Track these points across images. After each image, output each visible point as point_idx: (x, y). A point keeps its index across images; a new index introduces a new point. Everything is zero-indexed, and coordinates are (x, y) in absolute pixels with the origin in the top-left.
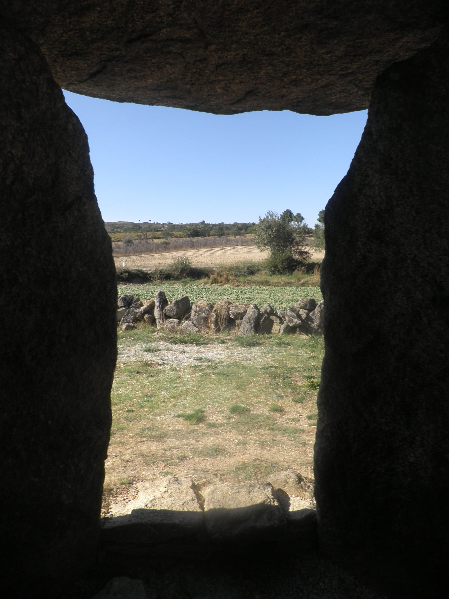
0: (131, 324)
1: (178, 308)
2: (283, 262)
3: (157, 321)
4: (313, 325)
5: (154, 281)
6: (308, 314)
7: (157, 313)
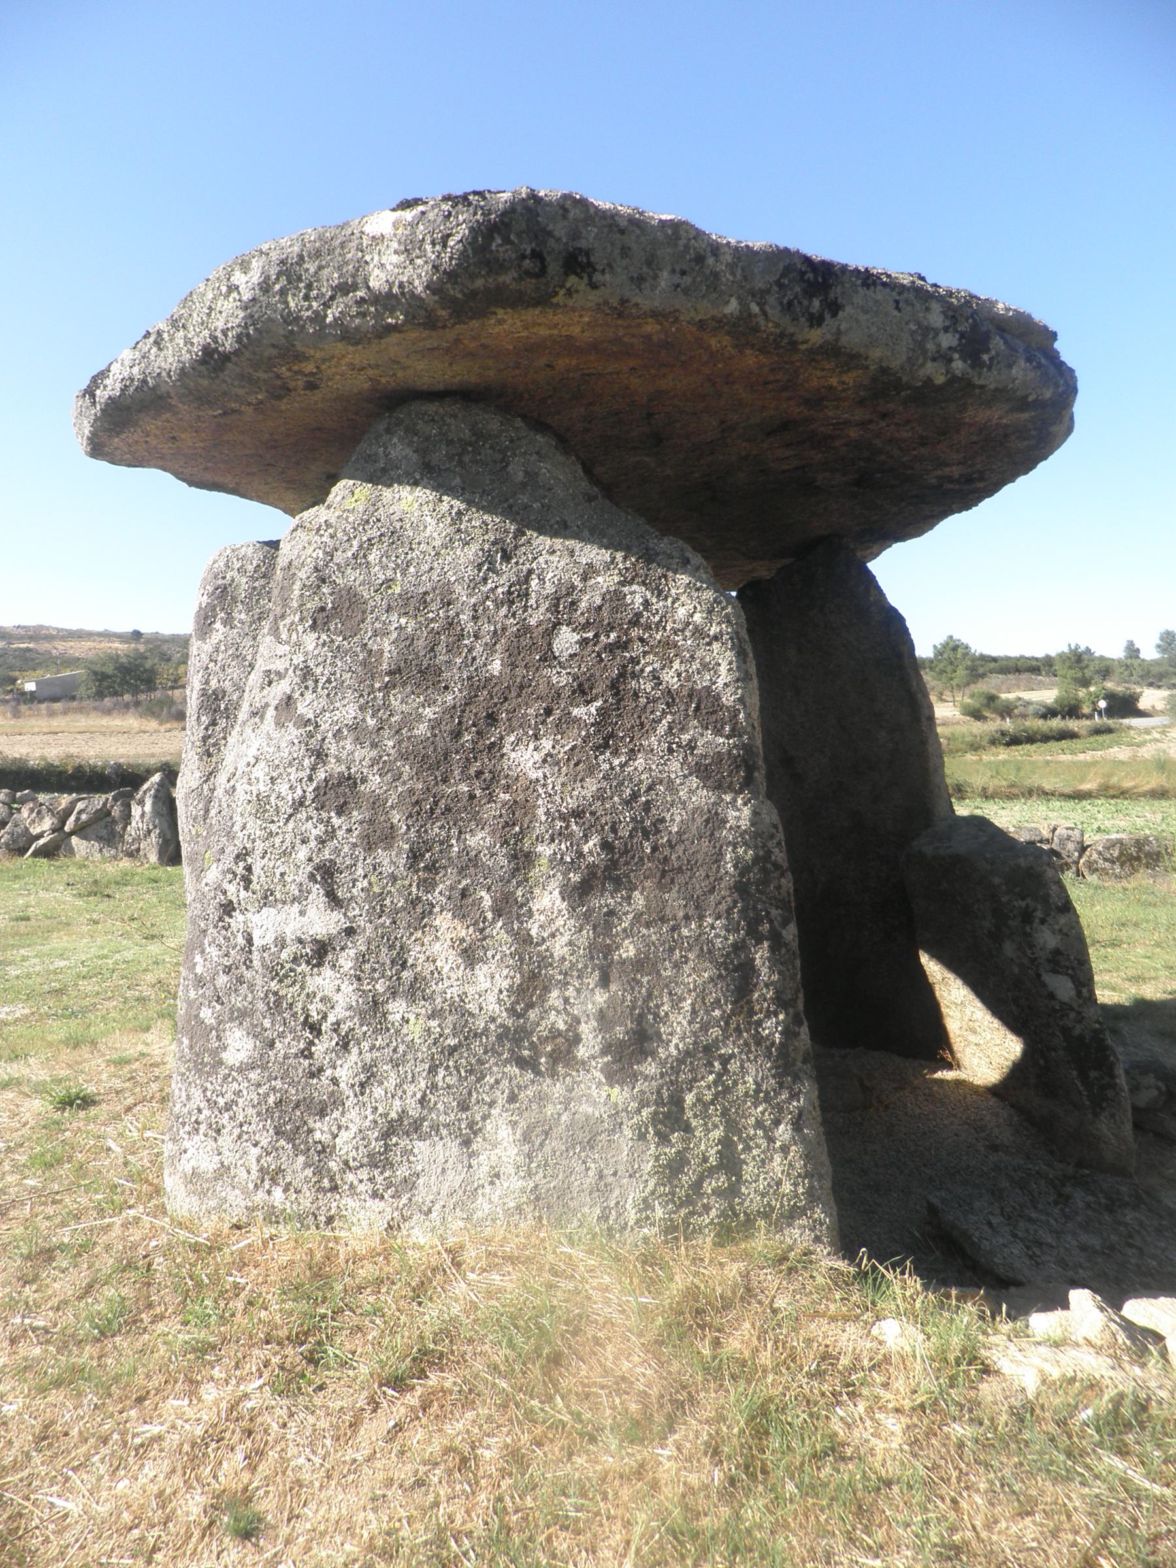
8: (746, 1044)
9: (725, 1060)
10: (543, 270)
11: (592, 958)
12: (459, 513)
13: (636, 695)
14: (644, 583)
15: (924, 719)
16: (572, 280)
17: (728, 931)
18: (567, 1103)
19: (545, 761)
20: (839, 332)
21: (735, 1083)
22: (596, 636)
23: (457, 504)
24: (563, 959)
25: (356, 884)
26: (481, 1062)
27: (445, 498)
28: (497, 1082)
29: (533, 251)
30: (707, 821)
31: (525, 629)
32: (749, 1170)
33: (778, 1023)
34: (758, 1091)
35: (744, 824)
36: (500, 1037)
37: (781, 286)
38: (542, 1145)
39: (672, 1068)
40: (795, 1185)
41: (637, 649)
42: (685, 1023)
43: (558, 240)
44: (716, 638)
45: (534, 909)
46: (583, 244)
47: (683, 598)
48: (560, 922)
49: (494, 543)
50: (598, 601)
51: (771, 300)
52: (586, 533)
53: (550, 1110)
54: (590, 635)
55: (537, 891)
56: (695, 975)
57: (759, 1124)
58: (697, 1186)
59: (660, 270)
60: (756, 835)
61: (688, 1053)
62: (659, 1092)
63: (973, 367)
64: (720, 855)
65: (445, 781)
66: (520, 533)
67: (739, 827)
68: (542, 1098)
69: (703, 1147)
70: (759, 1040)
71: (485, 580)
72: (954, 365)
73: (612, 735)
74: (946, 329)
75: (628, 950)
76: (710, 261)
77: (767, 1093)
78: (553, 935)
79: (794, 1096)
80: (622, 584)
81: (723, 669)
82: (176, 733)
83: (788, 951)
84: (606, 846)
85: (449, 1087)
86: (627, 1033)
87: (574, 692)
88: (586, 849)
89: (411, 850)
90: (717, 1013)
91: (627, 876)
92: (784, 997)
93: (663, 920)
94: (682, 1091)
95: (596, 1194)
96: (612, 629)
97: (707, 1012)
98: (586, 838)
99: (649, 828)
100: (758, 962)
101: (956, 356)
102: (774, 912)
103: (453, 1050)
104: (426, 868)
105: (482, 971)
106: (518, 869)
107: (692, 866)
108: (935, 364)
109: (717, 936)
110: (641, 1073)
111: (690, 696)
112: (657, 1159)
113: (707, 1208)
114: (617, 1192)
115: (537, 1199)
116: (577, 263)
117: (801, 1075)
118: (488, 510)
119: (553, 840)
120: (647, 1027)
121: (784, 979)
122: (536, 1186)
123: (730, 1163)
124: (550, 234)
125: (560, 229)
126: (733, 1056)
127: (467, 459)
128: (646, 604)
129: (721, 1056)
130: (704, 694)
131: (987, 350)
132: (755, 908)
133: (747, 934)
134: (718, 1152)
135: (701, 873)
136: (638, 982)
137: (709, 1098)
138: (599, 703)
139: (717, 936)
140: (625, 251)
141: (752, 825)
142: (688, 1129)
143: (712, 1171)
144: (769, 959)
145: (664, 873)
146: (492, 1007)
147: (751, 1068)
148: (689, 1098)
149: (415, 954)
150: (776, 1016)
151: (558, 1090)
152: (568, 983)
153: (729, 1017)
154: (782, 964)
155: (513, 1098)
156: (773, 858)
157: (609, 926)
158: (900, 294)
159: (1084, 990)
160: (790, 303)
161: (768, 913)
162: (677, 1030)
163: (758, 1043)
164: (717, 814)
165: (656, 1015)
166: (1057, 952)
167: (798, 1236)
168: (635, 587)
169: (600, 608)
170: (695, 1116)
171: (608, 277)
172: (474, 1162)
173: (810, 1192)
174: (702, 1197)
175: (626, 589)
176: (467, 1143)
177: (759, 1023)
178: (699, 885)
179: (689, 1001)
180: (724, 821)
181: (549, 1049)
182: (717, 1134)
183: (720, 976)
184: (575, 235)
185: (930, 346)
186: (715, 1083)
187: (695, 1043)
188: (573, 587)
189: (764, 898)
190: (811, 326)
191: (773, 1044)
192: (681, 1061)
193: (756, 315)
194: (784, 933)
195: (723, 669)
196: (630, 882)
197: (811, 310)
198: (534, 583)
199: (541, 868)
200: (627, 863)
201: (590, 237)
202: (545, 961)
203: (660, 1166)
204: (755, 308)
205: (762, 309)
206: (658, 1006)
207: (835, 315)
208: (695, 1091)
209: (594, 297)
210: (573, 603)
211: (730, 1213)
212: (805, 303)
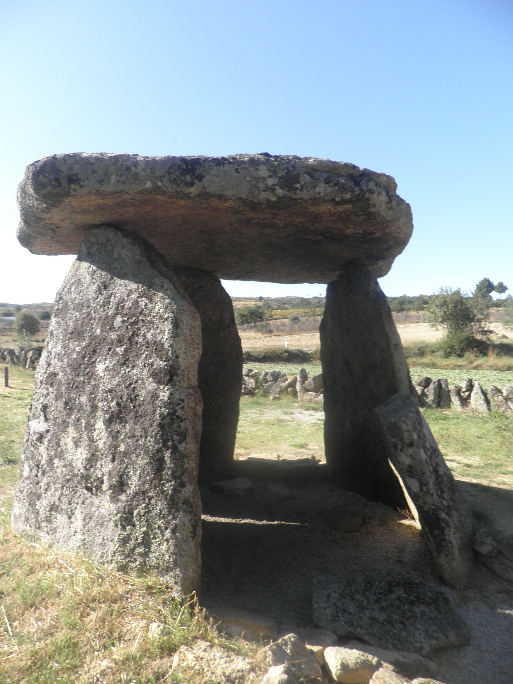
0: (277, 396)
1: (315, 383)
2: (461, 343)
3: (298, 394)
4: (427, 400)
5: (314, 362)
6: (423, 391)
7: (298, 387)
8: (158, 493)
9: (150, 498)
10: (60, 185)
11: (110, 450)
12: (95, 272)
13: (137, 343)
14: (146, 297)
15: (392, 347)
16: (73, 186)
18: (98, 507)
19: (106, 369)
20: (204, 187)
21: (153, 509)
22: (128, 319)
23: (95, 268)
24: (102, 449)
25: (52, 414)
26: (76, 487)
27: (92, 266)
28: (80, 495)
29: (54, 178)
30: (152, 396)
31: (107, 316)
32: (153, 547)
33: (171, 485)
34: (160, 513)
35: (166, 398)
36: (82, 477)
37: (169, 173)
38: (88, 523)
39: (131, 499)
40: (170, 557)
41: (141, 324)
42: (137, 480)
43: (64, 172)
44: (166, 319)
45: (96, 428)
46: (74, 172)
47: (159, 303)
48: (103, 434)
49: (102, 283)
50: (131, 305)
51: (165, 179)
52: (131, 277)
53: (93, 509)
54: (126, 319)
55: (98, 421)
56: (142, 461)
58: (133, 550)
59: (111, 176)
60: (170, 403)
61: (137, 493)
62: (124, 508)
63: (289, 191)
64: (155, 411)
65: (78, 376)
66: (112, 278)
67: (163, 400)
68: (92, 504)
69: (137, 534)
70: (163, 491)
71: (98, 297)
72: (277, 191)
73: (128, 360)
74: (270, 177)
75: (122, 448)
76: (133, 169)
77: (164, 515)
78: (100, 439)
79: (174, 518)
80: (138, 297)
81: (166, 333)
82: (267, 338)
83: (180, 454)
84: (118, 404)
85: (66, 495)
86: (116, 482)
87: (117, 342)
88: (112, 405)
89: (65, 402)
90: (148, 478)
91: (124, 417)
92: (175, 474)
93: (134, 436)
94: (133, 509)
95: (101, 546)
96: (134, 316)
97: (145, 477)
98: (112, 400)
99: (133, 399)
100: (166, 458)
101: (277, 187)
102: (175, 437)
103: (68, 480)
104: (69, 409)
105: (79, 450)
106: (92, 412)
107: (145, 415)
108: (266, 193)
109: (151, 445)
110: (120, 499)
111: (154, 343)
112: (119, 535)
113: (136, 560)
114: (108, 547)
115: (84, 544)
116: (72, 179)
117: (180, 509)
118: (103, 270)
119: (102, 401)
120: (124, 480)
121: (176, 467)
122: (84, 539)
123: (146, 542)
124: (60, 170)
125: (64, 168)
126: (152, 497)
127: (102, 250)
128: (146, 305)
129: (148, 496)
130: (159, 343)
131: (299, 182)
132: (167, 435)
133: (163, 446)
134: (142, 537)
135: (148, 418)
136: (124, 461)
137: (142, 513)
138: (124, 347)
139: (151, 445)
140: (94, 172)
141: (169, 399)
142: (134, 525)
143: (139, 545)
144: (170, 457)
145: (136, 417)
146: (80, 466)
147: (159, 503)
148: (135, 512)
149: (62, 443)
150: (171, 482)
151: (97, 501)
152: (102, 459)
153: (152, 480)
154: (176, 460)
155: (83, 503)
156: (177, 414)
157: (117, 437)
158: (238, 166)
159: (425, 488)
160: (175, 180)
161: (172, 437)
162: (134, 483)
163: (162, 493)
164: (156, 394)
165: (127, 476)
166: (411, 467)
167: (168, 579)
168: (143, 299)
169: (131, 308)
170: (137, 520)
171: (87, 182)
172: (71, 526)
173: (175, 562)
174: (133, 554)
175: (139, 300)
176: (70, 518)
177: (163, 484)
178: (147, 423)
179: (139, 472)
180: (158, 397)
181: (95, 484)
182: (144, 529)
183: (150, 462)
184: (70, 169)
185: (261, 185)
186: (145, 507)
187: (139, 489)
188: (124, 299)
189: (171, 431)
190: (188, 187)
191: (168, 494)
192: (134, 497)
193: (161, 186)
194: (179, 446)
195: (166, 333)
196: (126, 420)
197: (186, 181)
198: (113, 297)
199: (99, 413)
200: (125, 412)
201: (77, 169)
202: (96, 449)
203: (120, 539)
204: (159, 184)
205: (163, 184)
206: (128, 472)
207: (200, 180)
208: (138, 510)
209: (84, 191)
210: (123, 306)
211: (144, 564)
212: (183, 178)
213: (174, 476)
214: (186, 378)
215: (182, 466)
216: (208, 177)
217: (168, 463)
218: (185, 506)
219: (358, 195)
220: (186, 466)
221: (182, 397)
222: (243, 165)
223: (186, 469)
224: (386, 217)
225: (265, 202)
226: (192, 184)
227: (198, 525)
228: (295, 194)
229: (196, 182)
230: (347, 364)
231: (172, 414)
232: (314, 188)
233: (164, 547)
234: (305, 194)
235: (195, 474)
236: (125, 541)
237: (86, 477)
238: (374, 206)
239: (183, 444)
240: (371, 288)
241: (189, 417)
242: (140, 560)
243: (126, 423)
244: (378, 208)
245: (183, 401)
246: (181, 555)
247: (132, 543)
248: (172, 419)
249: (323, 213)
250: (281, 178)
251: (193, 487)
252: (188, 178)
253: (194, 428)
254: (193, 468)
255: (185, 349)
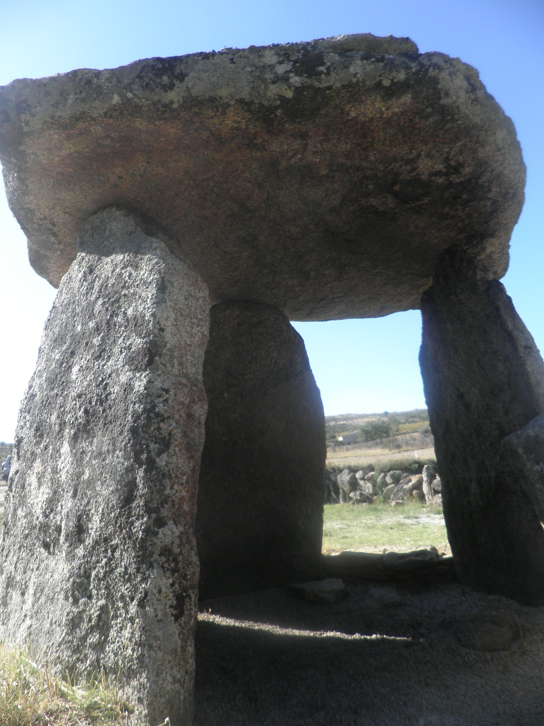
0: (401, 501)
3: (426, 497)
7: (425, 488)
8: (124, 538)
11: (72, 480)
13: (115, 325)
15: (521, 350)
17: (125, 459)
20: (188, 89)
21: (116, 567)
32: (113, 633)
33: (142, 524)
34: (126, 573)
40: (133, 650)
42: (98, 521)
57: (123, 597)
58: (83, 639)
59: (68, 95)
60: (148, 395)
62: (80, 568)
63: (309, 77)
66: (100, 259)
69: (92, 611)
72: (292, 81)
73: (104, 350)
74: (280, 63)
76: (95, 80)
77: (130, 575)
79: (144, 580)
83: (158, 473)
84: (86, 412)
90: (112, 515)
91: (93, 429)
92: (150, 505)
94: (90, 569)
101: (292, 75)
107: (116, 417)
108: (276, 85)
117: (155, 565)
120: (83, 523)
121: (152, 493)
123: (102, 625)
126: (117, 546)
129: (111, 546)
132: (140, 444)
133: (134, 462)
134: (98, 616)
136: (86, 495)
141: (145, 389)
148: (93, 574)
150: (142, 519)
153: (117, 518)
154: (151, 481)
156: (157, 410)
158: (234, 54)
160: (147, 85)
161: (148, 446)
162: (95, 525)
163: (130, 538)
164: (130, 385)
165: (88, 515)
167: (129, 693)
171: (39, 108)
173: (141, 659)
175: (123, 271)
177: (132, 523)
182: (102, 602)
183: (117, 490)
185: (269, 76)
187: (100, 535)
189: (146, 436)
190: (166, 91)
193: (132, 98)
194: (158, 460)
197: (163, 83)
200: (94, 421)
204: (130, 95)
206: (90, 510)
208: (97, 570)
210: (107, 286)
211: (96, 665)
212: (158, 81)
213: (149, 510)
214: (176, 362)
215: (161, 491)
216: (192, 75)
217: (142, 489)
218: (163, 559)
219: (417, 72)
220: (168, 491)
221: (166, 386)
222: (239, 54)
223: (168, 496)
224: (471, 116)
225: (278, 102)
226: (171, 86)
227: (189, 596)
228: (319, 81)
229: (177, 83)
230: (461, 396)
231: (150, 412)
232: (347, 67)
233: (126, 633)
234: (335, 80)
235: (186, 508)
236: (74, 623)
237: (44, 528)
238: (447, 94)
239: (164, 456)
240: (478, 277)
241: (177, 416)
242: (92, 657)
243: (94, 437)
244: (454, 98)
245: (167, 391)
246: (151, 647)
247: (85, 626)
248: (149, 418)
249: (371, 120)
250: (296, 62)
251: (181, 529)
252: (165, 79)
253: (185, 434)
254: (182, 499)
255: (176, 320)
